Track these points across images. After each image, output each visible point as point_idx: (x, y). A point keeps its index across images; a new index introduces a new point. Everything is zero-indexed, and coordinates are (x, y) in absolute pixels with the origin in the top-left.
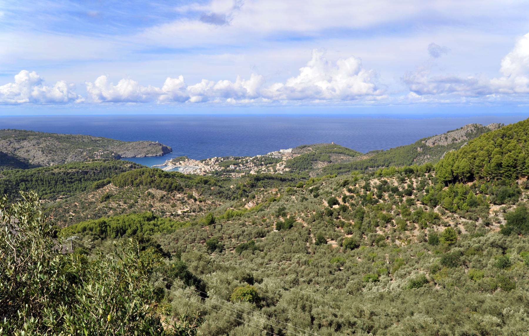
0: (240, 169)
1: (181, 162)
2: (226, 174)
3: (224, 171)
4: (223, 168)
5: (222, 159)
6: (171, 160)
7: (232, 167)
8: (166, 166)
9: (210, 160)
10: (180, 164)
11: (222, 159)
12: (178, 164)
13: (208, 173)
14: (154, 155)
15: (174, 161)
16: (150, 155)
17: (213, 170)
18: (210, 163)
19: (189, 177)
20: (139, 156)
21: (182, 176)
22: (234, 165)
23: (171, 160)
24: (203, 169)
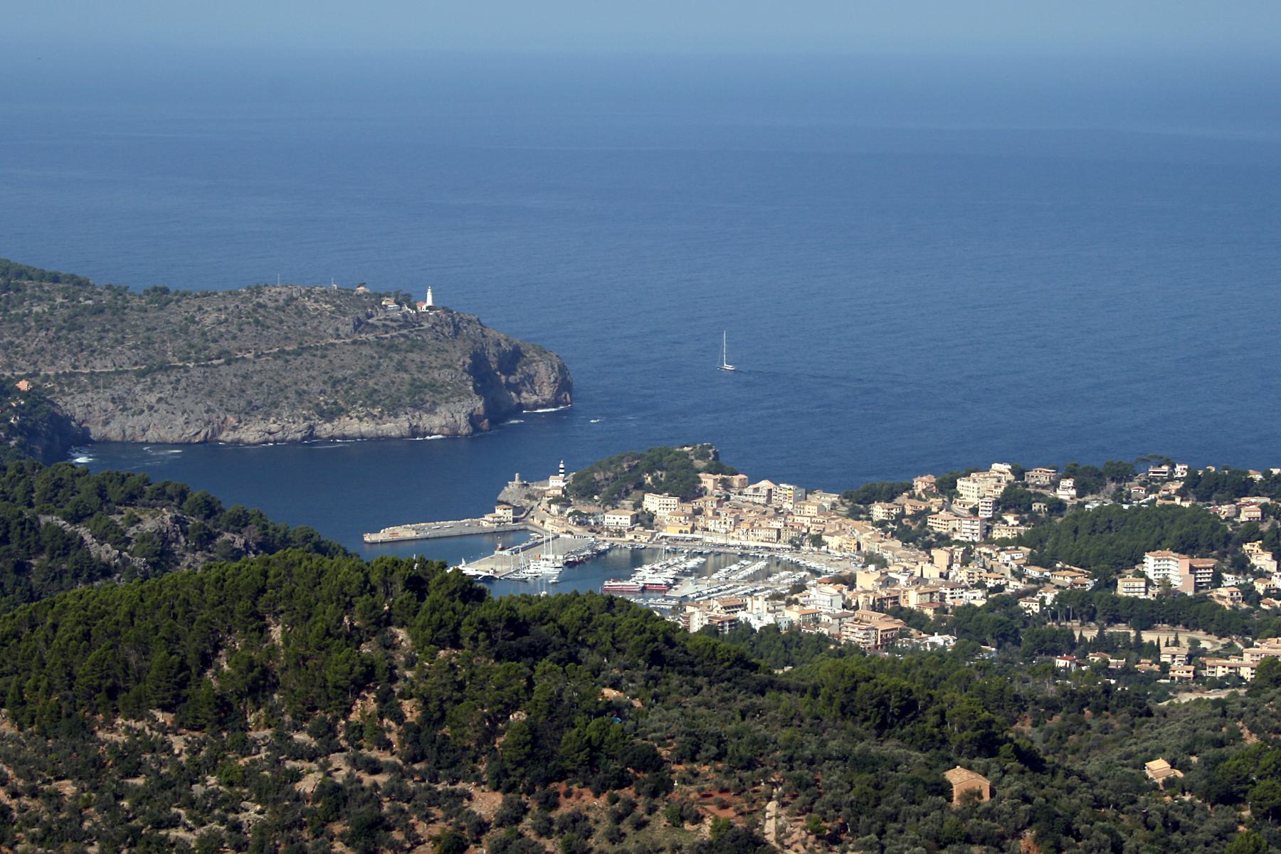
0: (1248, 593)
1: (652, 502)
2: (1103, 644)
3: (1074, 605)
4: (1065, 577)
5: (1066, 491)
6: (556, 484)
7: (1170, 570)
8: (517, 537)
9: (947, 489)
10: (646, 520)
11: (1066, 491)
12: (619, 518)
13: (913, 619)
14: (394, 427)
15: (583, 489)
16: (354, 426)
17: (977, 599)
18: (939, 524)
19: (737, 661)
20: (251, 433)
21: (663, 650)
22: (1186, 547)
23: (556, 484)
24: (867, 580)
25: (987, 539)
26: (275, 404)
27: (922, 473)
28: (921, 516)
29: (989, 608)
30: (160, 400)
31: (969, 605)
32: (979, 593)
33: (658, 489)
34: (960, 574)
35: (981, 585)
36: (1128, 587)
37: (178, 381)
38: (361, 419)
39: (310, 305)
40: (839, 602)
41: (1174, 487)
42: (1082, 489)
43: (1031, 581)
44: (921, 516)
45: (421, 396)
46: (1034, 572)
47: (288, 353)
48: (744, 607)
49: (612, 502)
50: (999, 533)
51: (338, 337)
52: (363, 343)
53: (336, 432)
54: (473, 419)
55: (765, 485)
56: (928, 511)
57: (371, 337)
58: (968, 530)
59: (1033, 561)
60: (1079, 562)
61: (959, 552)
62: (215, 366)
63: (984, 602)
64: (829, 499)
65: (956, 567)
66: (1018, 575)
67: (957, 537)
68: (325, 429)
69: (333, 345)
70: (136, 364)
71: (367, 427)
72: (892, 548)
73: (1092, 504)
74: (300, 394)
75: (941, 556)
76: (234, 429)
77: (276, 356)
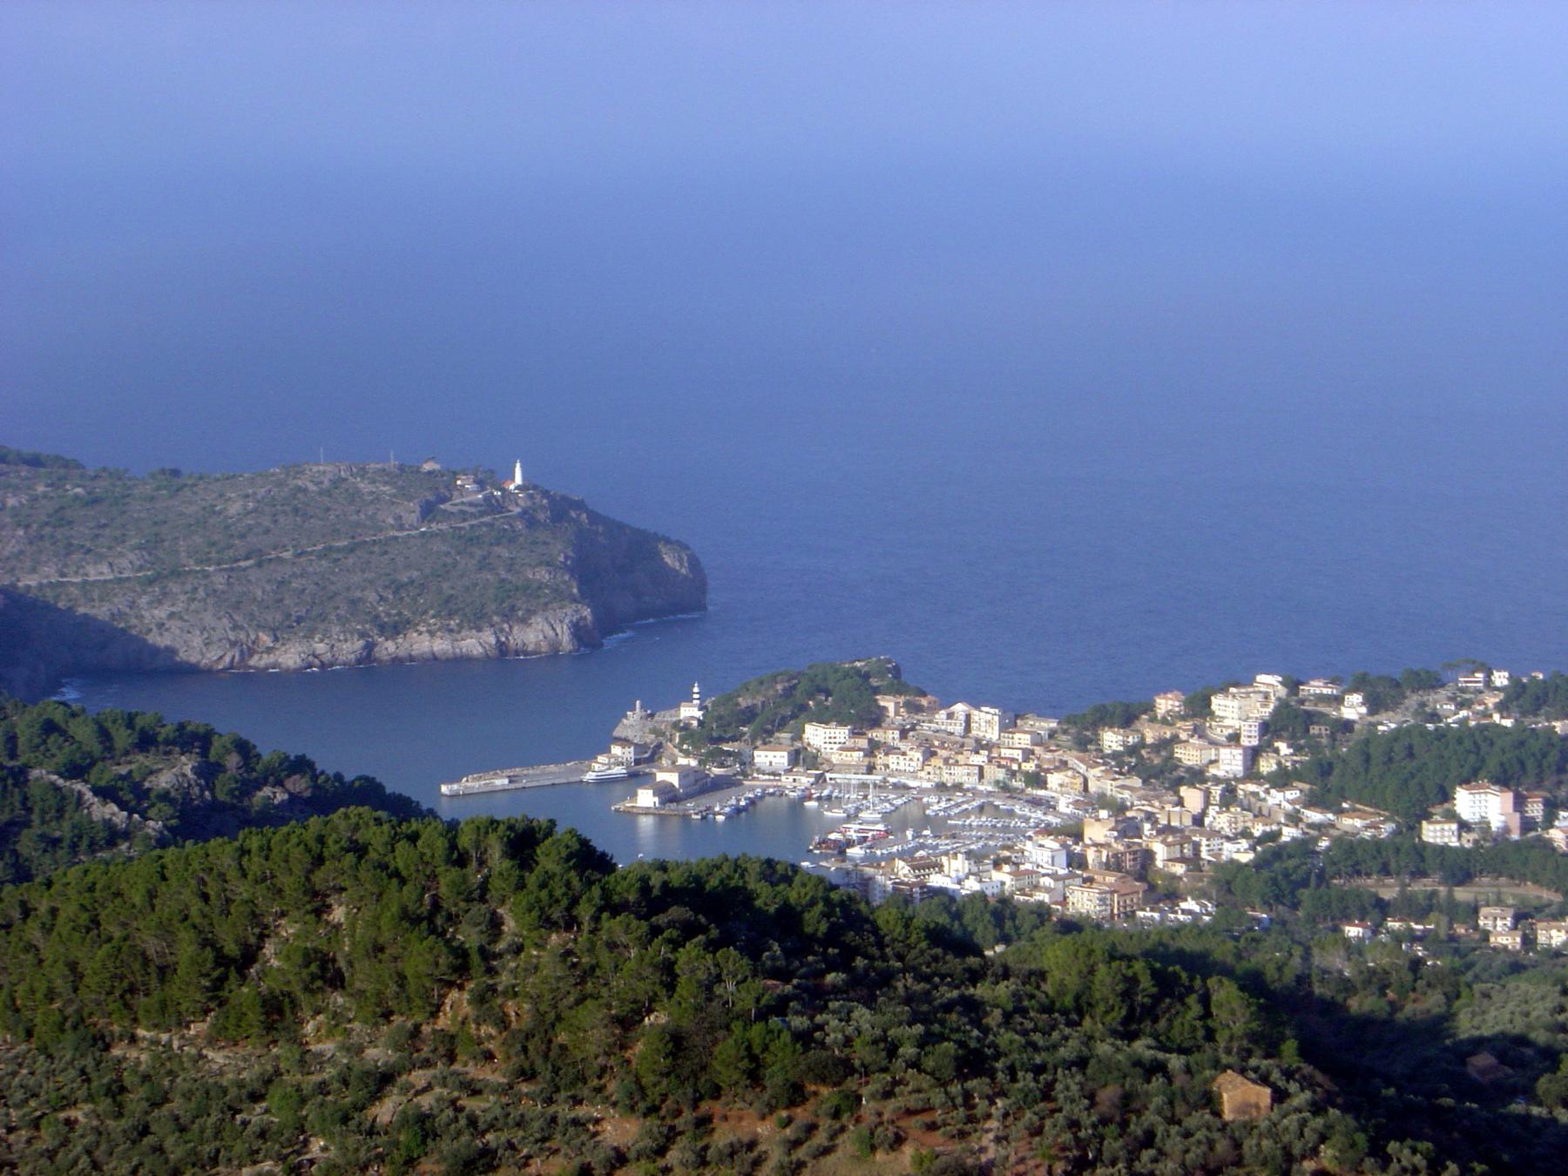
1: (816, 735)
5: (1353, 708)
9: (1199, 708)
11: (1353, 708)
12: (770, 758)
14: (475, 643)
16: (423, 643)
17: (1241, 853)
18: (1189, 755)
20: (290, 656)
23: (690, 712)
24: (1099, 831)
25: (1251, 774)
26: (323, 617)
27: (1164, 690)
28: (1167, 744)
29: (1259, 865)
30: (172, 615)
31: (1232, 861)
32: (1244, 844)
33: (822, 719)
34: (1219, 820)
35: (1246, 834)
36: (1436, 833)
37: (195, 590)
38: (432, 634)
39: (364, 486)
40: (1062, 858)
41: (1491, 700)
42: (1375, 704)
43: (1311, 826)
44: (1167, 744)
45: (514, 604)
46: (1314, 816)
47: (339, 550)
48: (939, 867)
49: (765, 736)
50: (1267, 765)
51: (401, 528)
52: (434, 535)
53: (402, 653)
54: (578, 630)
55: (960, 708)
56: (1175, 739)
57: (444, 526)
58: (1230, 762)
59: (1312, 802)
60: (1372, 799)
61: (1216, 791)
62: (245, 569)
63: (1251, 856)
64: (1047, 725)
65: (1212, 811)
66: (1294, 819)
67: (1213, 771)
68: (388, 648)
69: (396, 538)
70: (141, 568)
71: (441, 645)
72: (1127, 789)
73: (1387, 724)
74: (354, 602)
75: (1192, 798)
76: (269, 650)
77: (323, 555)
